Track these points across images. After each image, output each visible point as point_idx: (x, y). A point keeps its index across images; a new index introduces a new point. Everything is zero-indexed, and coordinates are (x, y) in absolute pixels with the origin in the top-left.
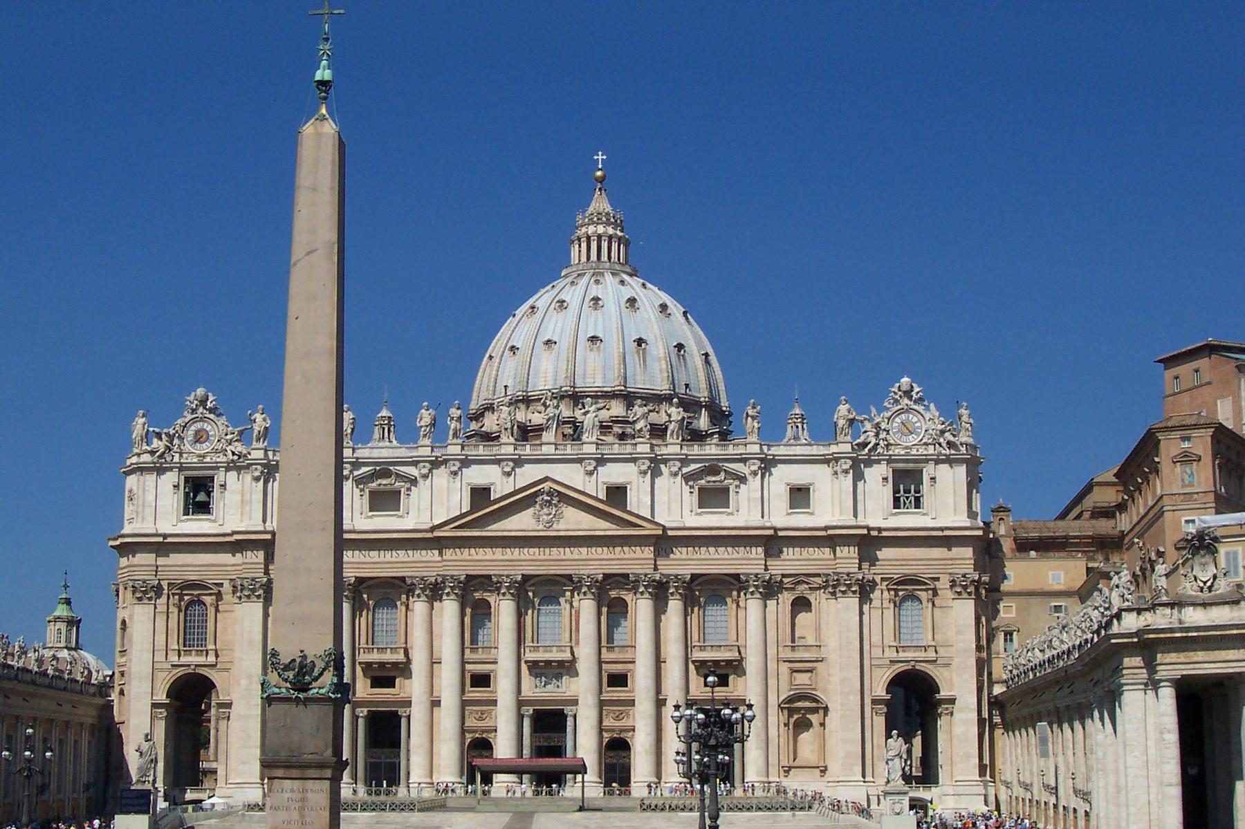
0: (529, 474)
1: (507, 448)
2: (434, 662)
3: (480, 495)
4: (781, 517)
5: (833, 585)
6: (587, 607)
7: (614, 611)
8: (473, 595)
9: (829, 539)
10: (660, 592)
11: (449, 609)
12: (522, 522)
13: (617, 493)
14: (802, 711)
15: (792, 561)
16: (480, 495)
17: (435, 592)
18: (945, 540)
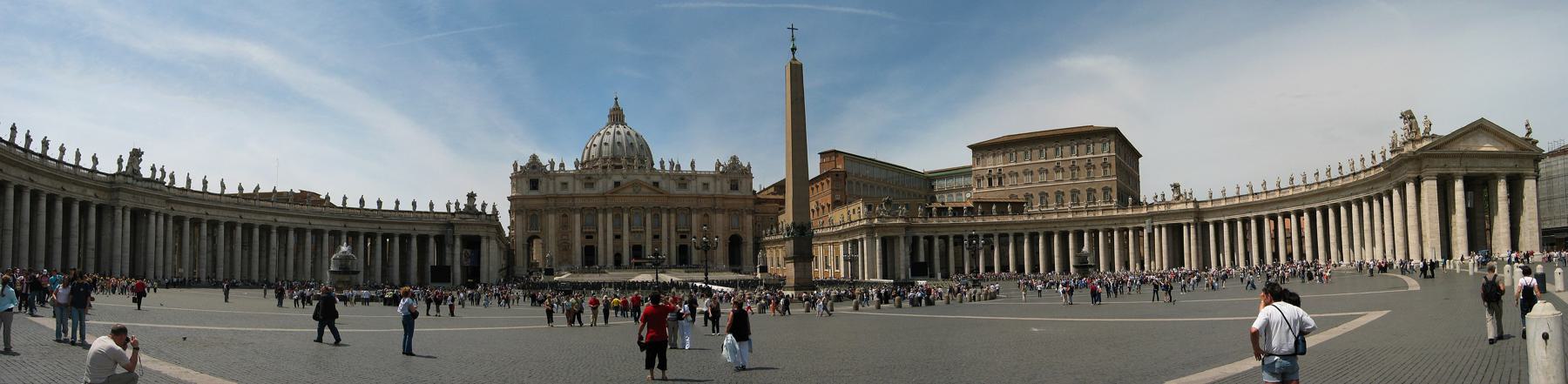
0: (631, 177)
1: (624, 170)
2: (605, 231)
3: (617, 184)
4: (701, 191)
5: (714, 210)
6: (649, 216)
7: (657, 217)
8: (618, 212)
9: (714, 197)
10: (669, 211)
11: (610, 216)
12: (630, 190)
13: (656, 184)
14: (706, 248)
15: (705, 204)
16: (617, 184)
17: (605, 211)
18: (744, 198)
